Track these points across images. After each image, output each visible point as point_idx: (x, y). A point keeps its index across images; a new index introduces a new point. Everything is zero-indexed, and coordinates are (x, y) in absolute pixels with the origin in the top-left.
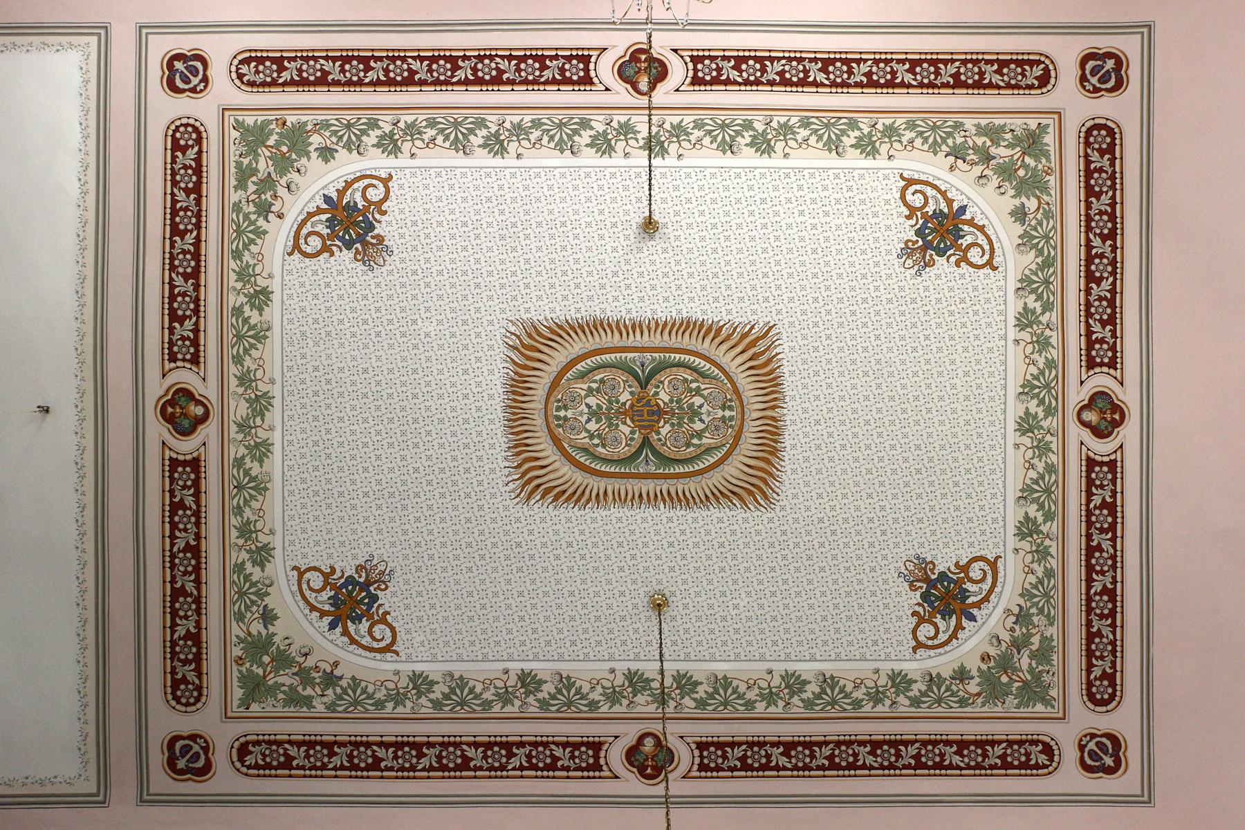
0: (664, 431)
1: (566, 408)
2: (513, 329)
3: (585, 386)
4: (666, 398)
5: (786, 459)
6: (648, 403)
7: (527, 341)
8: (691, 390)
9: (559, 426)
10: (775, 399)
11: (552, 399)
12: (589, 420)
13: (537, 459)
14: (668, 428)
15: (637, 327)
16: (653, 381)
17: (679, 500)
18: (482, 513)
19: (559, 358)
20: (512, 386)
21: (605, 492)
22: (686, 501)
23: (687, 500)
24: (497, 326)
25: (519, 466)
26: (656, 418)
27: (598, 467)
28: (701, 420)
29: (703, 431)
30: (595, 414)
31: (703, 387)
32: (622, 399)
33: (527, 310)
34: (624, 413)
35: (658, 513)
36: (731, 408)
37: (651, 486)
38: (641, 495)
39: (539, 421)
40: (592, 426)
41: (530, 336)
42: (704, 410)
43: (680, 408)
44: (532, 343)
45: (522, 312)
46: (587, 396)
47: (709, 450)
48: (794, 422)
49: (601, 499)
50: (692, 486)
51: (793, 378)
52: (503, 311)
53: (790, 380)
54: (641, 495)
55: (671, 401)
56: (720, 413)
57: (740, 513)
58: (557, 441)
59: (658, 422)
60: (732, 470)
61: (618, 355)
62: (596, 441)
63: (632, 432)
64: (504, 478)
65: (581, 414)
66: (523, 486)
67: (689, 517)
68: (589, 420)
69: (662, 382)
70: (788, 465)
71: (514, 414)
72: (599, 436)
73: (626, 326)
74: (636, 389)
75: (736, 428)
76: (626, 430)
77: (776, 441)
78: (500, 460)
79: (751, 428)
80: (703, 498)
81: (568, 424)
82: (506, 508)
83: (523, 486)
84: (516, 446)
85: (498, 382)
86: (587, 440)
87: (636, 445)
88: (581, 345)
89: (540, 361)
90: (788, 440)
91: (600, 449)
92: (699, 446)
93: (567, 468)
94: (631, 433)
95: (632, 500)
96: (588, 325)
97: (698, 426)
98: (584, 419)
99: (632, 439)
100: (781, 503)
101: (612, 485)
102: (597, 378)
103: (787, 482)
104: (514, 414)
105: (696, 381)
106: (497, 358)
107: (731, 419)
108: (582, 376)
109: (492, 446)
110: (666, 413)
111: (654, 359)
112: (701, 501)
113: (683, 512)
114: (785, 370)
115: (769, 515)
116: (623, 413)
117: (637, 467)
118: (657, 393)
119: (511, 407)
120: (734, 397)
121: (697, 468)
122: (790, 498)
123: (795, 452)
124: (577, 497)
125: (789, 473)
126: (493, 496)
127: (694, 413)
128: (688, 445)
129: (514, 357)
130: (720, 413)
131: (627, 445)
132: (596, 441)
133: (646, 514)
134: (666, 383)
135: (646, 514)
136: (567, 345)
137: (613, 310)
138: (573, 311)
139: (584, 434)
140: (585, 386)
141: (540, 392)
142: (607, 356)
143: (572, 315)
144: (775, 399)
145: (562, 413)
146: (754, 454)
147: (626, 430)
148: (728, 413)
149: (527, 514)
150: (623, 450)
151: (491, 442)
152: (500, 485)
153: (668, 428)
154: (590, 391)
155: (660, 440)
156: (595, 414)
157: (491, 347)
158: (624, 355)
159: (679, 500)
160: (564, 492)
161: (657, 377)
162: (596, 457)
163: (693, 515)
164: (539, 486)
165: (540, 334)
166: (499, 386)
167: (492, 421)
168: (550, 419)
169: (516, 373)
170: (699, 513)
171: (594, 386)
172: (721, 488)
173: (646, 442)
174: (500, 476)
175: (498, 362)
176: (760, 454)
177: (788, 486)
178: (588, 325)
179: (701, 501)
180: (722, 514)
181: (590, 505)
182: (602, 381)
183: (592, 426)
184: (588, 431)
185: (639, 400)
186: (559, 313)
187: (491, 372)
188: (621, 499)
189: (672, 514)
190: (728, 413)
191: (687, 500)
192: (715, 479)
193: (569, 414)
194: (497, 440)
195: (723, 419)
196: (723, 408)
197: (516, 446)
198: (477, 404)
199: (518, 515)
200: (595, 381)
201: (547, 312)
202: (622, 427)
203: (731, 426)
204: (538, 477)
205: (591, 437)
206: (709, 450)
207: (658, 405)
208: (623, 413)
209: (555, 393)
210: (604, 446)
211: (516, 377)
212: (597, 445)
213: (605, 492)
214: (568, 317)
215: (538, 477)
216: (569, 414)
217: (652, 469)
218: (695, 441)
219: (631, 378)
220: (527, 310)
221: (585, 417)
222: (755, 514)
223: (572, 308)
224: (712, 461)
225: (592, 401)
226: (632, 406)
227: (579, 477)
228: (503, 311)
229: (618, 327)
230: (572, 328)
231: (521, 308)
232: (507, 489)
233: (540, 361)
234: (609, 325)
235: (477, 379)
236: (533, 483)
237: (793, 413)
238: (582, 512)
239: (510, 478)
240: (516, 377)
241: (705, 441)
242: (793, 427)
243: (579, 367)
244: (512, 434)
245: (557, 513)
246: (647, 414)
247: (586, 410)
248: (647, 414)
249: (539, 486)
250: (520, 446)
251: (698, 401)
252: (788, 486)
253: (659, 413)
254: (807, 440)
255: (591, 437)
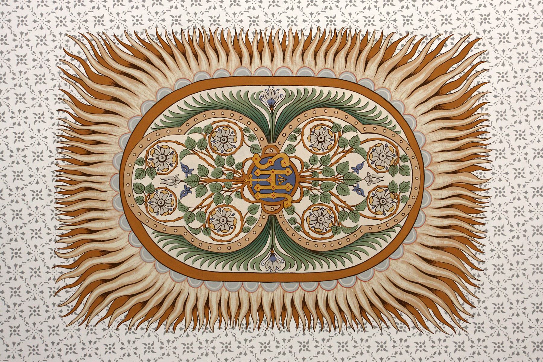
0: (300, 208)
1: (152, 172)
2: (75, 50)
3: (182, 139)
4: (306, 156)
5: (486, 249)
6: (278, 165)
7: (97, 68)
8: (344, 143)
9: (140, 201)
10: (474, 156)
11: (131, 159)
12: (187, 191)
13: (104, 253)
14: (306, 202)
15: (265, 44)
16: (286, 130)
17: (320, 316)
18: (16, 339)
19: (143, 95)
20: (70, 139)
21: (207, 304)
22: (328, 316)
23: (332, 315)
24: (52, 45)
25: (77, 264)
26: (288, 186)
27: (197, 265)
28: (358, 190)
29: (359, 207)
30: (196, 181)
31: (362, 137)
32: (238, 158)
33: (99, 21)
34: (240, 180)
35: (286, 335)
36: (404, 171)
37: (278, 293)
38: (261, 308)
39: (110, 193)
40: (191, 201)
41: (101, 60)
42: (362, 174)
43: (327, 171)
44: (103, 72)
45: (91, 24)
46: (185, 154)
47: (368, 237)
48: (500, 192)
49: (200, 314)
50: (340, 293)
51: (503, 123)
52: (61, 22)
53: (497, 125)
54: (261, 308)
55: (313, 160)
56: (387, 179)
57: (412, 336)
58: (136, 225)
59: (292, 193)
60: (403, 267)
61: (235, 90)
62: (196, 224)
63: (252, 210)
64: (52, 283)
65: (175, 182)
66: (82, 295)
67: (333, 342)
68: (187, 191)
69: (300, 131)
70: (489, 260)
71: (72, 182)
72: (201, 216)
73: (248, 45)
74: (261, 142)
75: (412, 202)
76: (242, 205)
77: (472, 222)
78: (47, 256)
79: (434, 201)
80: (357, 312)
81: (154, 198)
82: (54, 331)
83: (82, 295)
84: (72, 234)
85: (50, 134)
86: (182, 223)
87: (257, 229)
88: (179, 74)
89: (115, 99)
90: (490, 220)
91: (201, 237)
92: (354, 230)
93: (150, 266)
94: (250, 210)
95: (247, 316)
96: (191, 43)
97: (353, 199)
98: (178, 190)
99: (251, 221)
100: (477, 319)
101: (217, 292)
102: (202, 125)
103: (486, 287)
104: (72, 182)
105: (353, 128)
106: (50, 95)
107: (404, 187)
108: (179, 122)
109: (36, 233)
110: (305, 179)
111: (289, 95)
112: (354, 317)
113: (325, 334)
114: (491, 110)
115: (457, 338)
116: (239, 179)
117: (256, 264)
118: (292, 149)
119: (67, 172)
120: (410, 153)
121: (348, 264)
122: (490, 311)
123: (501, 239)
124: (162, 312)
125: (490, 272)
126: (35, 311)
127: (348, 179)
128: (336, 228)
129: (75, 94)
130: (387, 179)
131: (243, 230)
132: (196, 224)
133: (269, 338)
134: (307, 132)
135: (269, 338)
136: (157, 74)
137: (229, 19)
138: (169, 21)
139: (178, 213)
140: (182, 139)
141: (113, 149)
142: (219, 91)
143: (167, 27)
144: (474, 156)
145: (146, 181)
146: (438, 242)
147: (242, 205)
148: (399, 179)
149: (86, 340)
150: (238, 238)
151: (35, 226)
152: (46, 294)
153: (306, 202)
154: (190, 146)
155: (294, 221)
156: (196, 181)
157: (40, 79)
158: (244, 89)
159: (320, 316)
160: (144, 304)
161: (294, 123)
162: (195, 250)
163: (340, 338)
164: (105, 295)
165: (116, 58)
166: (50, 140)
167: (37, 195)
168: (128, 190)
169: (77, 119)
170: (349, 336)
171: (197, 137)
172: (384, 295)
173: (272, 225)
174: (47, 281)
175: (51, 101)
176: (446, 243)
177: (488, 292)
178: (191, 43)
179: (354, 317)
180: (385, 337)
181: (182, 325)
182: (209, 131)
183: (191, 201)
184: (184, 209)
185: (263, 160)
186: (147, 24)
187: (40, 118)
188: (231, 315)
189: (308, 337)
190: (399, 179)
191: (332, 315)
192: (376, 281)
193: (157, 181)
194: (48, 222)
195: (392, 188)
196: (393, 170)
197: (72, 234)
198: (16, 168)
199: (70, 342)
200: (199, 131)
201: (129, 23)
202: (237, 202)
203: (403, 199)
204: (105, 281)
205: (189, 217)
206: (368, 237)
207: (292, 167)
208: (239, 179)
209: (136, 150)
210: (207, 231)
211: (78, 126)
212: (198, 230)
213: (207, 304)
214: (161, 31)
215: (105, 281)
216: (157, 181)
217: (280, 266)
218: (348, 223)
219: (254, 125)
220: (99, 21)
221: (181, 187)
222: (435, 337)
223: (167, 17)
224: (372, 253)
225: (192, 161)
226: (253, 168)
227: (168, 281)
228: (61, 22)
229: (236, 45)
230: (167, 47)
231: (90, 17)
232: (57, 300)
233: (115, 99)
234: (223, 43)
235: (17, 129)
236: (96, 291)
237: (503, 180)
238: (170, 336)
239: (62, 284)
240: (78, 126)
241: (362, 222)
242: (500, 200)
243: (174, 108)
244: (68, 213)
245: (131, 337)
246: (275, 181)
247: (183, 176)
248: (275, 181)
249: (105, 295)
250: (79, 232)
251: (353, 159)
252: (488, 292)
253: (294, 179)
254: (521, 220)
255: (189, 217)
